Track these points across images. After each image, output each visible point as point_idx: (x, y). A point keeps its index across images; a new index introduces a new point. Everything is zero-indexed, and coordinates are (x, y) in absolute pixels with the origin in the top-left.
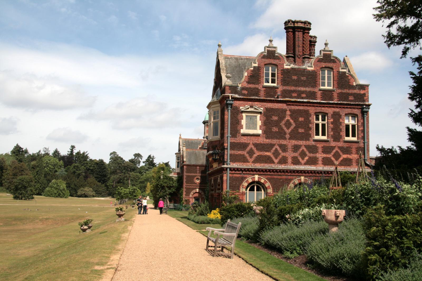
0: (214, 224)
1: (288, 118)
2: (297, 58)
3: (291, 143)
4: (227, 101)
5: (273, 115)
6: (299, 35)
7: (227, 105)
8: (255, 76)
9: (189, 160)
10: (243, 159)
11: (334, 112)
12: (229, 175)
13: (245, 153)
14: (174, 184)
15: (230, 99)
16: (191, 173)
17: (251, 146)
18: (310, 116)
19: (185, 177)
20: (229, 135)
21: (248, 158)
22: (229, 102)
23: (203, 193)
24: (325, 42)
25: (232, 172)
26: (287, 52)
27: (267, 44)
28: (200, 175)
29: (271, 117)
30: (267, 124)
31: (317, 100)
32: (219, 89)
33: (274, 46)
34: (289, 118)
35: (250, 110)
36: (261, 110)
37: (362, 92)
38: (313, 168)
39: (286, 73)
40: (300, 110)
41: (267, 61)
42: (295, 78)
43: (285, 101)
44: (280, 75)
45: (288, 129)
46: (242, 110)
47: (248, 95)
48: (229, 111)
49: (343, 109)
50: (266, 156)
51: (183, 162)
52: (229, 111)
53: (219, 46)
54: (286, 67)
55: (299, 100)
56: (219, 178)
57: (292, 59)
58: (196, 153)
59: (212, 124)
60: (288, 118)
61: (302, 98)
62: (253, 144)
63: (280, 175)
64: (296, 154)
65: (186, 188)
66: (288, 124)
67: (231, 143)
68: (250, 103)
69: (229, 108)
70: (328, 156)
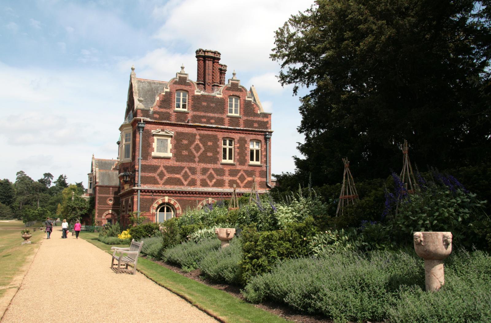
0: (124, 244)
1: (197, 142)
2: (207, 85)
4: (139, 124)
5: (183, 139)
6: (209, 63)
7: (139, 128)
8: (167, 101)
9: (102, 181)
11: (240, 138)
12: (139, 196)
13: (155, 175)
14: (86, 206)
15: (142, 122)
16: (104, 194)
17: (162, 168)
18: (218, 141)
19: (97, 198)
20: (140, 157)
21: (159, 180)
22: (140, 125)
23: (116, 215)
24: (233, 72)
25: (142, 194)
26: (198, 79)
27: (179, 70)
28: (113, 196)
29: (181, 141)
30: (177, 148)
31: (224, 125)
32: (131, 112)
33: (186, 73)
34: (199, 142)
35: (161, 133)
36: (172, 133)
37: (265, 120)
38: (220, 190)
39: (196, 99)
40: (209, 135)
41: (179, 87)
42: (205, 104)
43: (195, 126)
44: (190, 101)
45: (197, 152)
46: (153, 133)
47: (159, 119)
48: (141, 134)
49: (249, 135)
50: (175, 178)
51: (96, 183)
52: (141, 134)
53: (133, 69)
54: (196, 93)
55: (208, 125)
56: (130, 200)
57: (203, 86)
58: (109, 174)
59: (124, 146)
60: (197, 142)
61: (211, 124)
62: (164, 167)
63: (189, 197)
64: (204, 177)
65: (98, 209)
66: (198, 148)
67: (142, 165)
68: (162, 126)
69: (141, 131)
70: (234, 178)
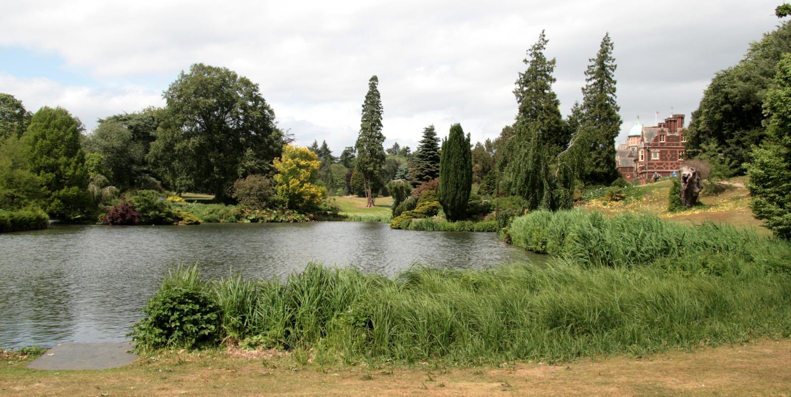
1: (669, 153)
3: (670, 162)
10: (653, 168)
30: (661, 156)
60: (669, 153)
